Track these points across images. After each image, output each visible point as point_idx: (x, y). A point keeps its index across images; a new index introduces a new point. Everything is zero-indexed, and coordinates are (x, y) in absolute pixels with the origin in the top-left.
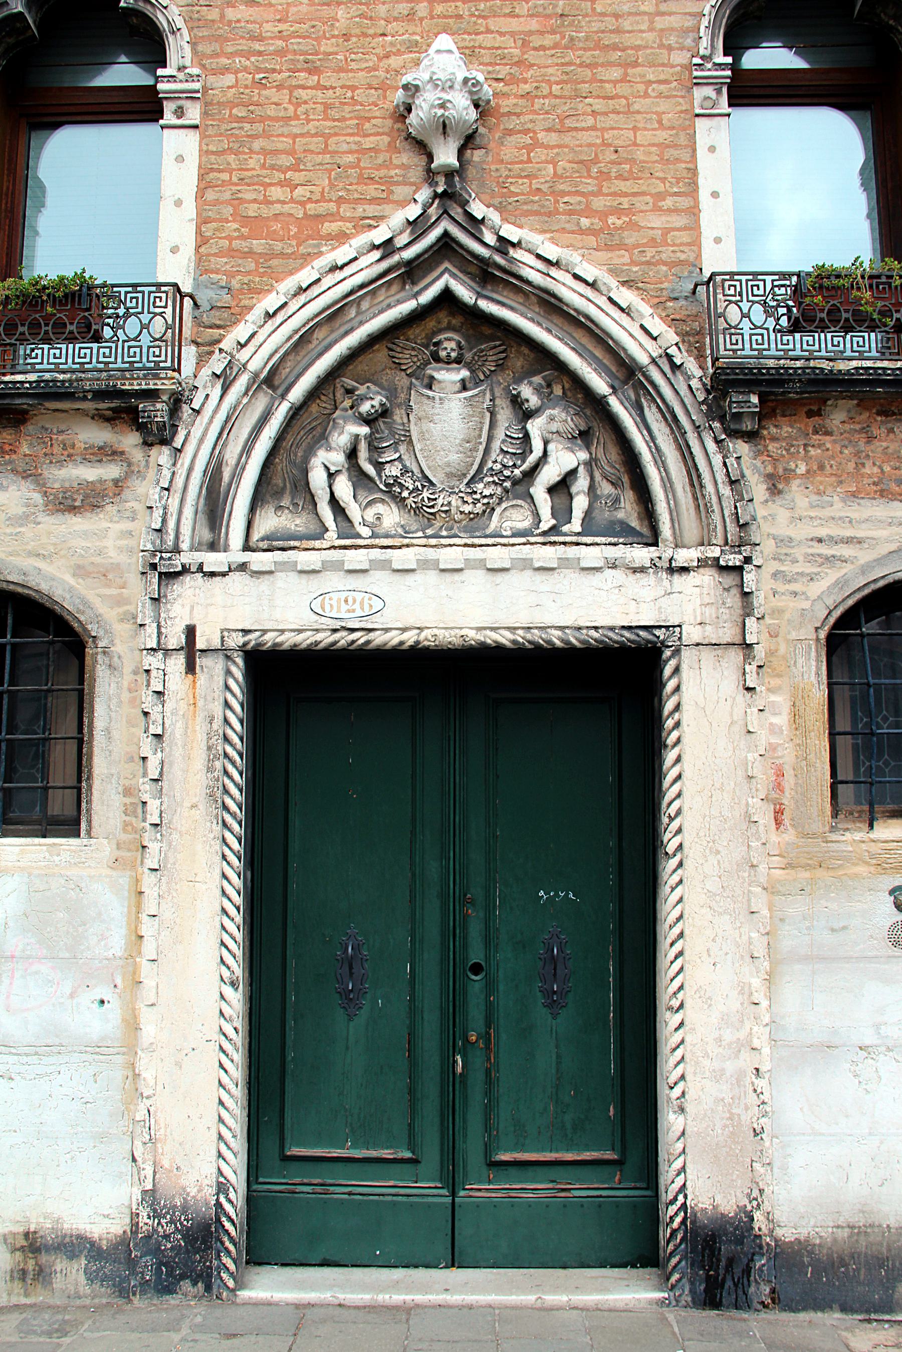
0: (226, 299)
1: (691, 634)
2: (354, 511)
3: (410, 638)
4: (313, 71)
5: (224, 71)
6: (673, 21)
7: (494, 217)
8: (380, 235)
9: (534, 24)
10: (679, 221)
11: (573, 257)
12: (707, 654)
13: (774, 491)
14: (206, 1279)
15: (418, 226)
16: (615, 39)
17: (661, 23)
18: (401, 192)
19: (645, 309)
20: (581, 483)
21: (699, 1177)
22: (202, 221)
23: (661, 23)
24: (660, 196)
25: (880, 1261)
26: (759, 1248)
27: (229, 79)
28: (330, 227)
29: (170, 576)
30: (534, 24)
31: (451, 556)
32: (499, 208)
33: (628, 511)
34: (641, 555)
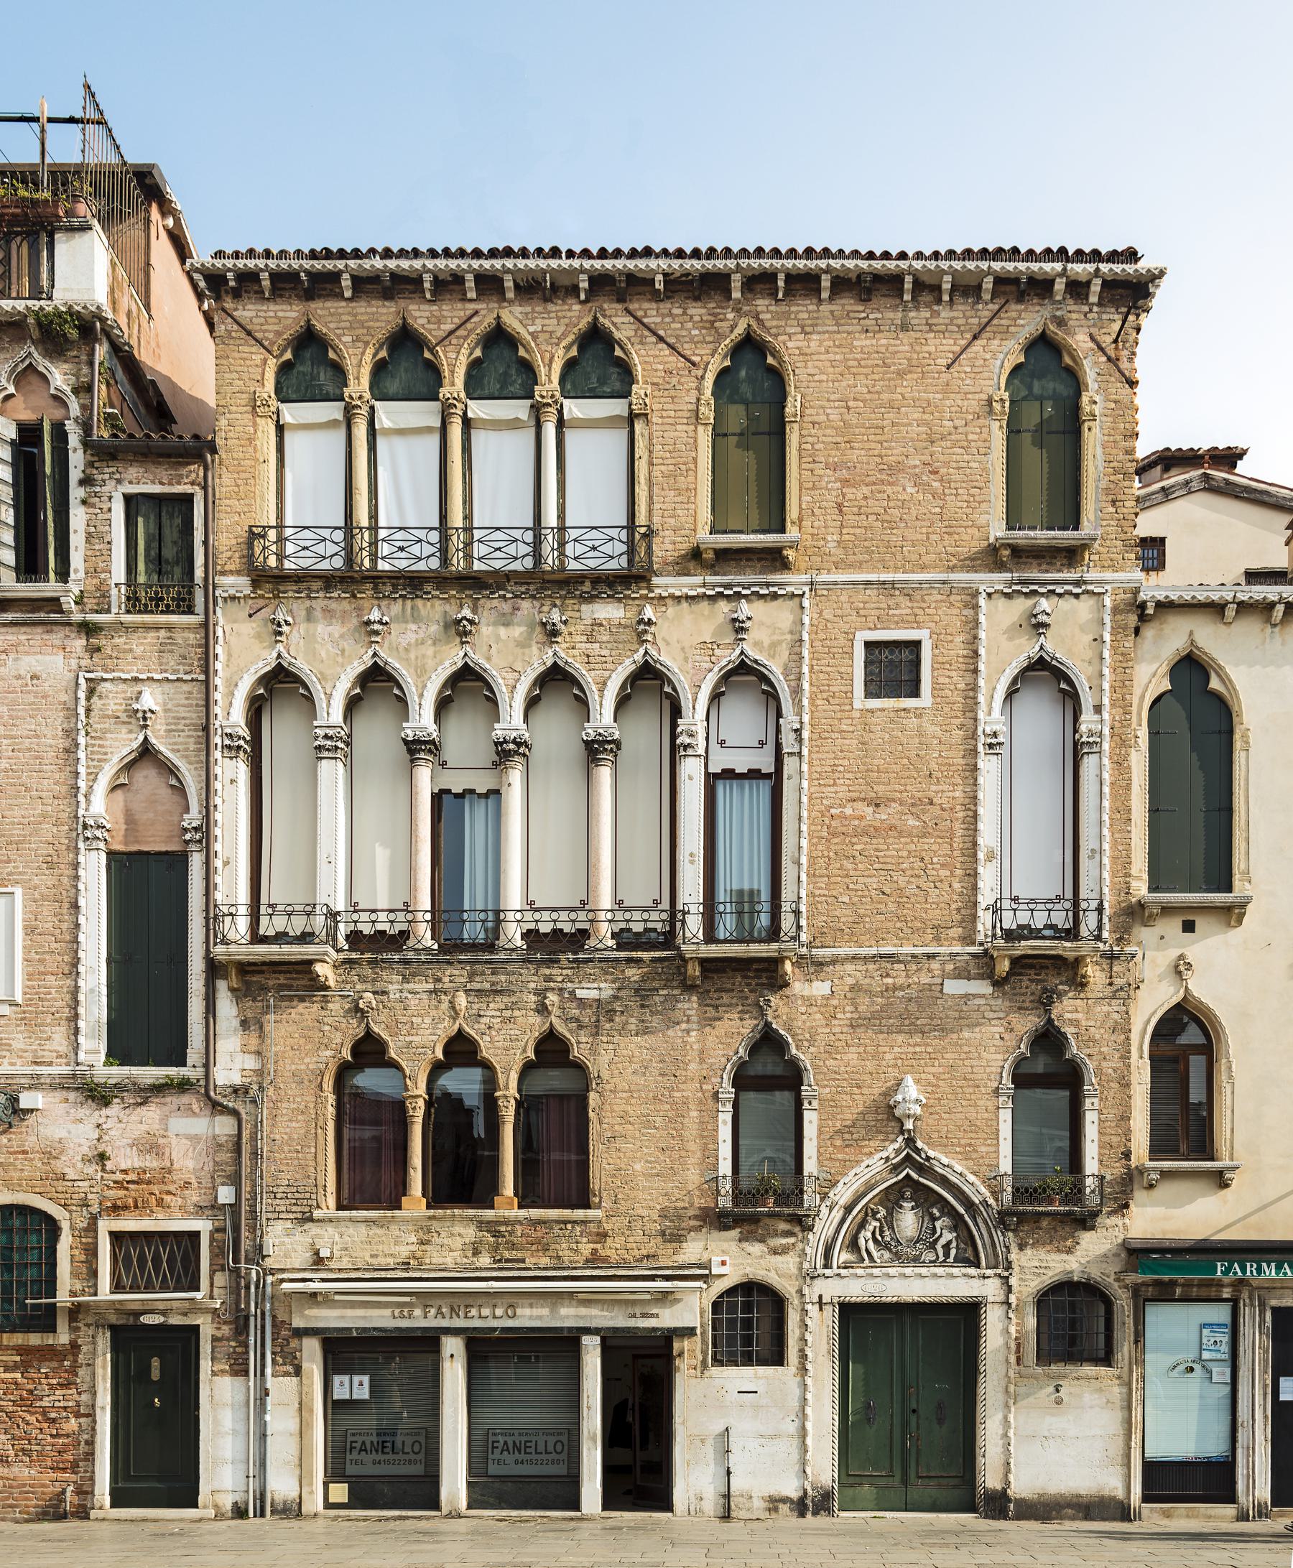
0: (830, 1177)
1: (991, 1299)
2: (875, 1254)
3: (895, 1299)
4: (859, 1087)
5: (825, 1086)
6: (994, 1069)
7: (926, 1148)
8: (884, 1154)
9: (941, 1070)
10: (992, 1149)
11: (953, 1163)
12: (996, 1306)
13: (1021, 1249)
14: (830, 1511)
15: (898, 1152)
16: (971, 1076)
17: (988, 1070)
18: (892, 1137)
19: (978, 1183)
20: (954, 1244)
21: (990, 1479)
22: (819, 1147)
23: (988, 1070)
24: (985, 1139)
25: (1048, 1505)
26: (1009, 1500)
27: (828, 1090)
28: (867, 1150)
29: (812, 1278)
30: (941, 1070)
31: (908, 1271)
32: (928, 1144)
33: (969, 1254)
34: (972, 1271)
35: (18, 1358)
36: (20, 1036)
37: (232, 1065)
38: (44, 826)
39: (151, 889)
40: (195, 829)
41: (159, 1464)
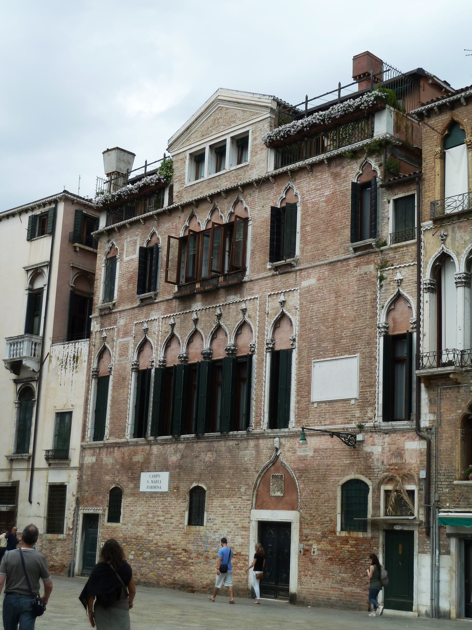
35: (355, 542)
36: (357, 412)
37: (426, 420)
38: (367, 329)
39: (399, 349)
40: (414, 323)
41: (399, 590)
